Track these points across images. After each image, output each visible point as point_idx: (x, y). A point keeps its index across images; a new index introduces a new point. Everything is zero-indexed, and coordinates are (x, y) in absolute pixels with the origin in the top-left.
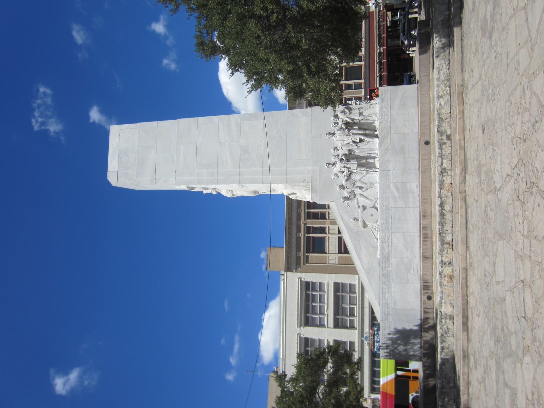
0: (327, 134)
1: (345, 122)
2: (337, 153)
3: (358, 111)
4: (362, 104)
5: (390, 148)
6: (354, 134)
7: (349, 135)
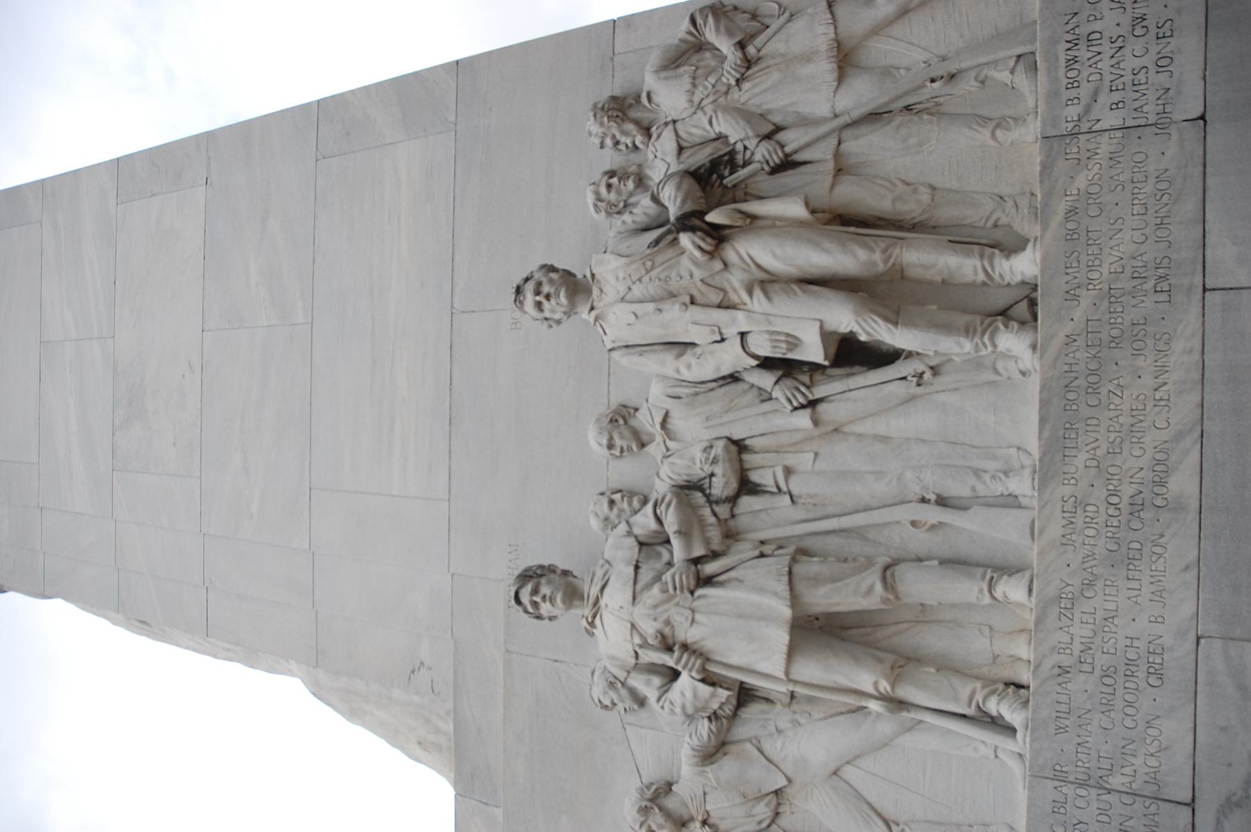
1: (700, 158)
2: (627, 471)
5: (1183, 483)
6: (767, 282)
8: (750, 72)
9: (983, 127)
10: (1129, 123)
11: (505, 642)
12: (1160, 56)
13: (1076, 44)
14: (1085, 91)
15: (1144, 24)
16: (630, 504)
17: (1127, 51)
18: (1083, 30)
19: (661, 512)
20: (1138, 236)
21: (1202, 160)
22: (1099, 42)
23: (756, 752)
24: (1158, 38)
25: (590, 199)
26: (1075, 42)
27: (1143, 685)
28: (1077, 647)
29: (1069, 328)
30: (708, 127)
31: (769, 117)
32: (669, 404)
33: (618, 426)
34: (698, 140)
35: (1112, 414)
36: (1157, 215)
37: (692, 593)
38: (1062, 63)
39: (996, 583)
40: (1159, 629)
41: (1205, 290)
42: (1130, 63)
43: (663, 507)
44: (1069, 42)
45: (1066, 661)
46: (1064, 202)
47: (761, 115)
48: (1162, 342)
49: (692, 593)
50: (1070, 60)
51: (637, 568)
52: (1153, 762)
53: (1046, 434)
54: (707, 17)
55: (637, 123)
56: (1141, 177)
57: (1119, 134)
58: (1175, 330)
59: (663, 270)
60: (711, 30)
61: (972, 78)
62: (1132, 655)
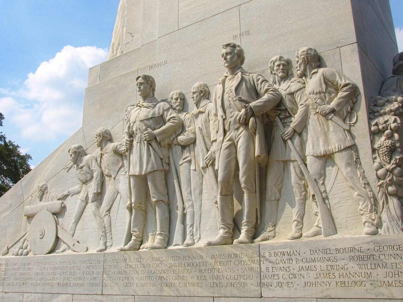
0: (228, 45)
1: (288, 104)
3: (334, 146)
4: (378, 160)
5: (167, 291)
6: (233, 146)
7: (227, 128)
8: (321, 117)
9: (298, 216)
10: (262, 274)
11: (140, 69)
12: (282, 283)
13: (289, 255)
14: (273, 259)
15: (293, 278)
16: (177, 106)
17: (284, 272)
18: (293, 257)
19: (171, 120)
20: (229, 277)
21: (249, 297)
22: (289, 263)
23: (120, 166)
24: (288, 283)
25: (274, 59)
26: (290, 255)
27: (124, 282)
28: (130, 263)
29: (204, 256)
30: (300, 104)
31: (304, 129)
32: (207, 112)
33: (200, 94)
34: (296, 100)
35: (183, 270)
36: (234, 283)
37: (145, 140)
38: (283, 251)
39: (161, 235)
40: (135, 286)
41: (214, 297)
42: (281, 273)
43: (172, 121)
44: (290, 252)
45: (127, 261)
46: (239, 253)
47: (306, 125)
48: (200, 285)
49: (145, 140)
50: (284, 253)
51: (151, 118)
52: (109, 285)
53: (178, 251)
54: (347, 91)
55: (305, 70)
56: (245, 278)
57: (259, 270)
58: (203, 289)
59: (233, 105)
60: (341, 95)
61: (316, 211)
62: (130, 278)
